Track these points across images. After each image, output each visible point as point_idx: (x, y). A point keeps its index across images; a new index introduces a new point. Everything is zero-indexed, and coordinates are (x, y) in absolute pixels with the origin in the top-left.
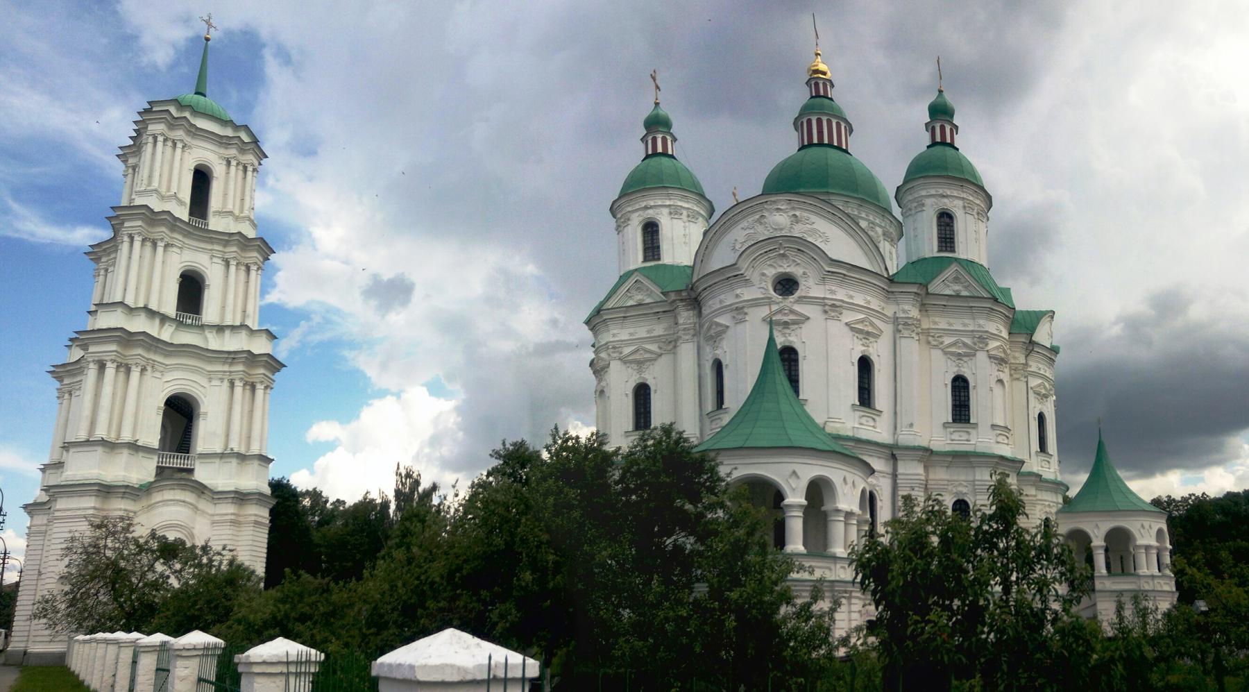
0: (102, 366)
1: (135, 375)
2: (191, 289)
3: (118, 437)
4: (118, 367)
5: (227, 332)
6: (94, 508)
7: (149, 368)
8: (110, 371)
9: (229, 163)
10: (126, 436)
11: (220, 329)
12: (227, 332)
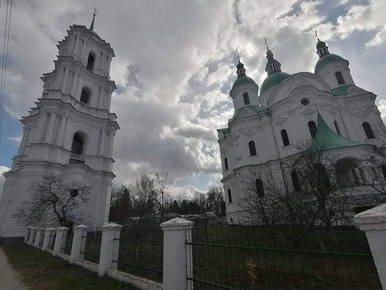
0: (49, 115)
1: (64, 120)
2: (86, 95)
3: (55, 143)
4: (56, 116)
5: (100, 112)
6: (43, 172)
7: (69, 119)
8: (53, 117)
9: (102, 54)
10: (59, 144)
11: (97, 110)
12: (100, 112)
